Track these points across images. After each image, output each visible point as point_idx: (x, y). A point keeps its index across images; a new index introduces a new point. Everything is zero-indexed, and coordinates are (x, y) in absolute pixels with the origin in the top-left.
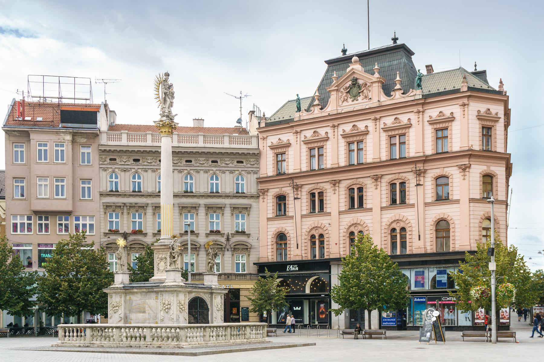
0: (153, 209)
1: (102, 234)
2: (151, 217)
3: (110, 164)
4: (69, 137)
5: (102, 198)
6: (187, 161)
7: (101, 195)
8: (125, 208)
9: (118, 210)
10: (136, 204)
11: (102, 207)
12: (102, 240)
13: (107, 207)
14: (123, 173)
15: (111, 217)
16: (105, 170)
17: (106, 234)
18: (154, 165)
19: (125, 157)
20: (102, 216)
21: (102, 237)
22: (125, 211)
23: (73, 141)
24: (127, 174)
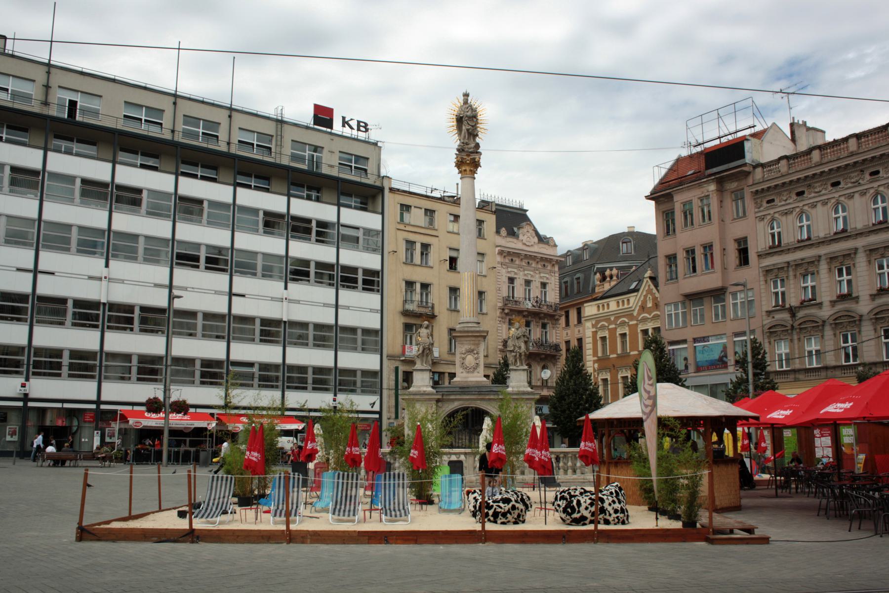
0: (828, 263)
1: (764, 313)
2: (827, 275)
3: (767, 209)
4: (712, 187)
5: (762, 260)
6: (872, 174)
7: (760, 256)
8: (790, 269)
9: (782, 275)
10: (802, 259)
11: (761, 274)
12: (765, 323)
13: (768, 271)
14: (784, 218)
15: (776, 287)
16: (762, 219)
17: (769, 313)
18: (824, 195)
19: (785, 193)
20: (763, 287)
21: (764, 318)
22: (791, 273)
23: (720, 190)
24: (790, 217)
